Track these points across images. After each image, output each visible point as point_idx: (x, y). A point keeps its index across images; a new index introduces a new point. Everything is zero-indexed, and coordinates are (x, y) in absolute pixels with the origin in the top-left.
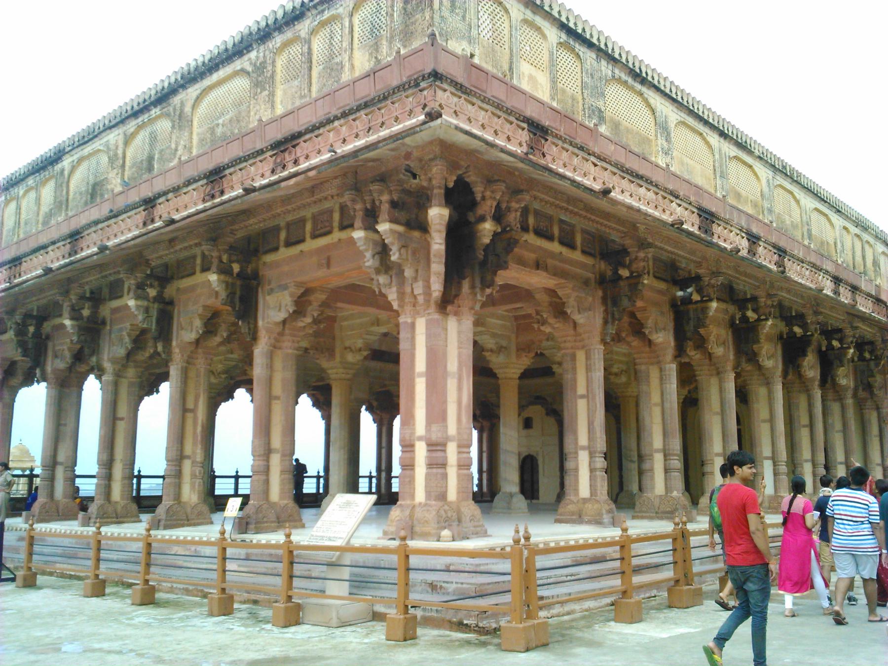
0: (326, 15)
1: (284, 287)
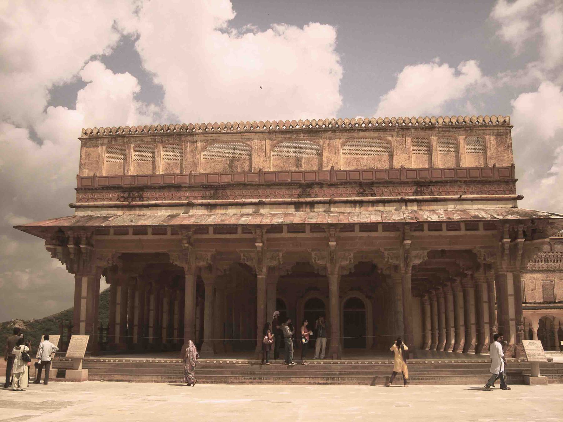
0: (447, 134)
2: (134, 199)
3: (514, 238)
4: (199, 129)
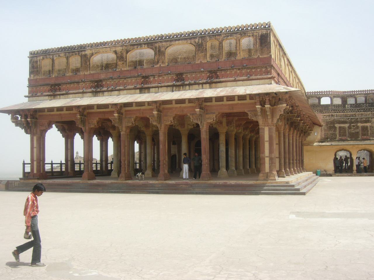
1: (214, 113)
2: (56, 91)
3: (263, 104)
4: (89, 47)
